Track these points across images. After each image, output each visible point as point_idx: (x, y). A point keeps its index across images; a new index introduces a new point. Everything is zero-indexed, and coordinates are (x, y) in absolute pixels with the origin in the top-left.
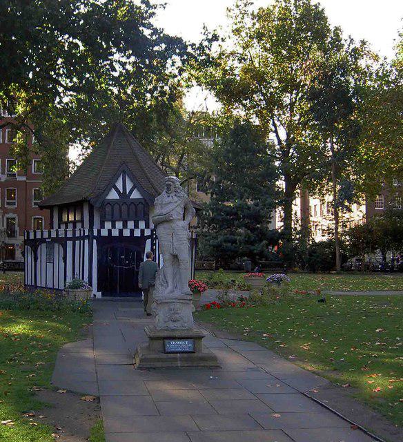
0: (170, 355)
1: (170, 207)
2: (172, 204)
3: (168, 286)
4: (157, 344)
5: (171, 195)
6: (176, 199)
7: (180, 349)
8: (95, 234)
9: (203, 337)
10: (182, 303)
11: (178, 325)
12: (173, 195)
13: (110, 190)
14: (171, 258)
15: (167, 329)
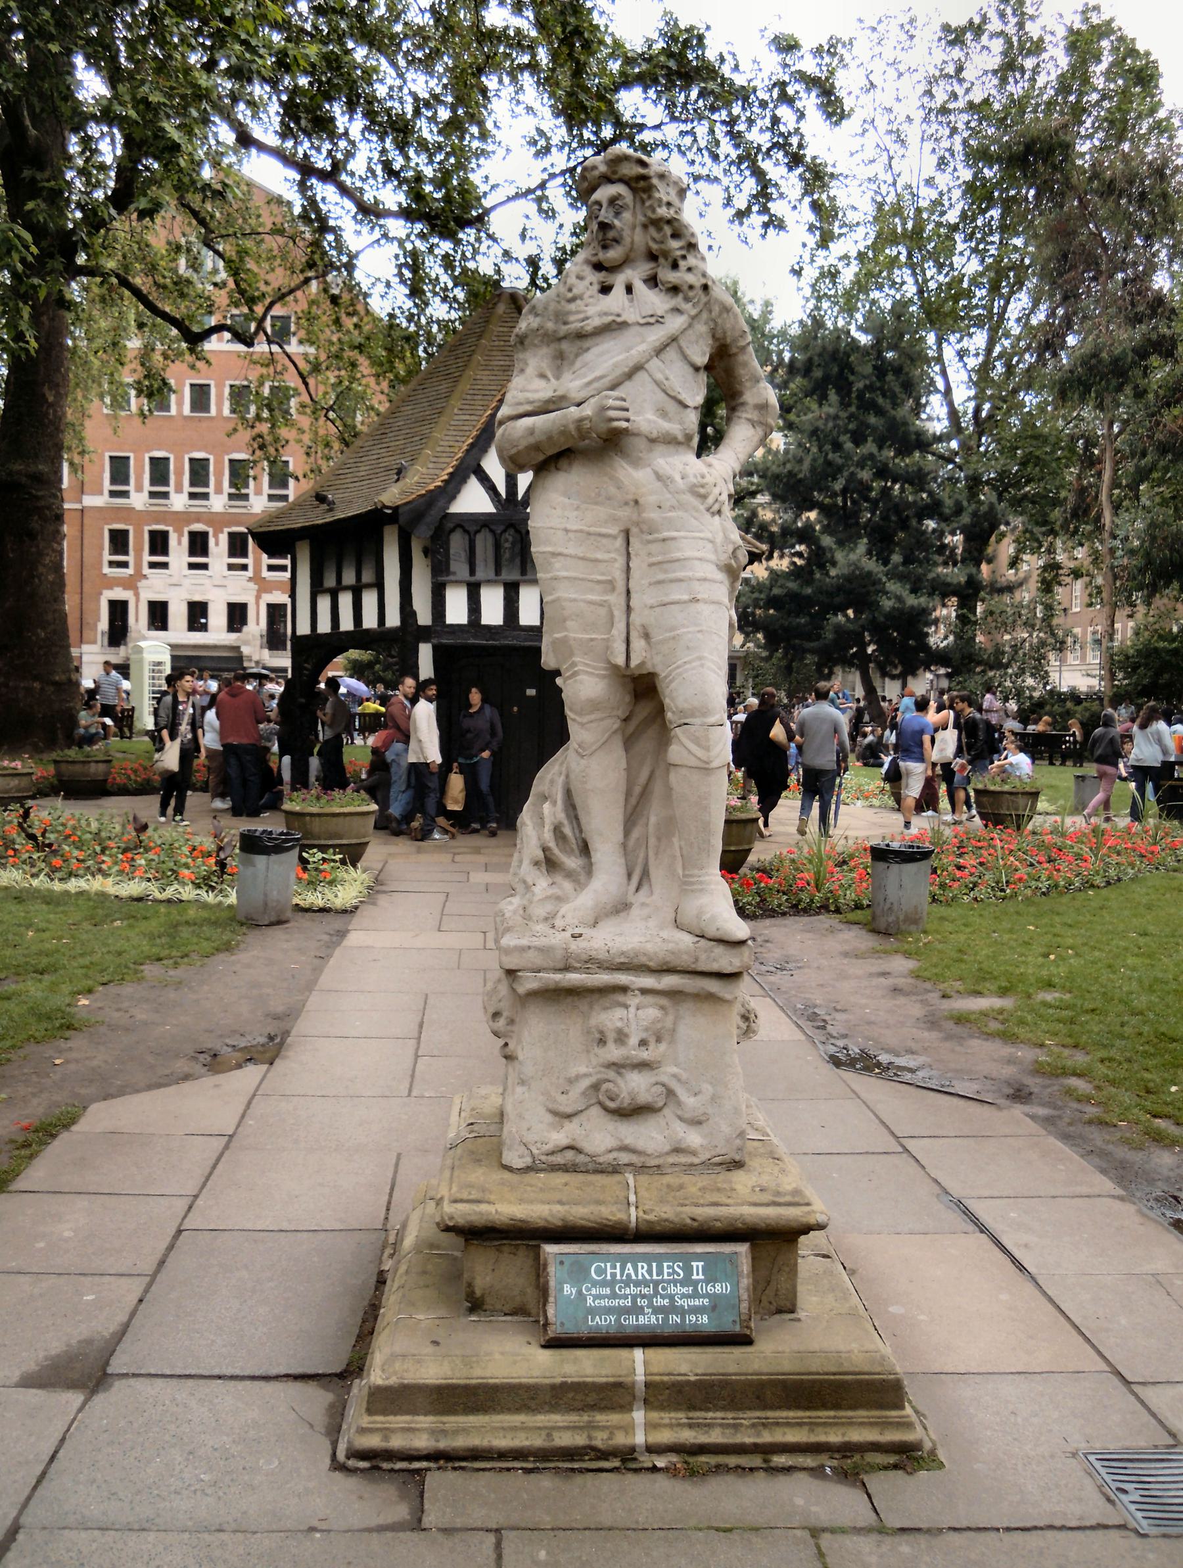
0: (586, 1366)
1: (606, 358)
2: (628, 336)
3: (589, 870)
4: (491, 1272)
5: (619, 281)
6: (654, 301)
7: (648, 1320)
8: (424, 617)
9: (806, 1229)
10: (674, 995)
11: (649, 1136)
12: (635, 275)
13: (464, 480)
14: (621, 700)
15: (571, 1162)
